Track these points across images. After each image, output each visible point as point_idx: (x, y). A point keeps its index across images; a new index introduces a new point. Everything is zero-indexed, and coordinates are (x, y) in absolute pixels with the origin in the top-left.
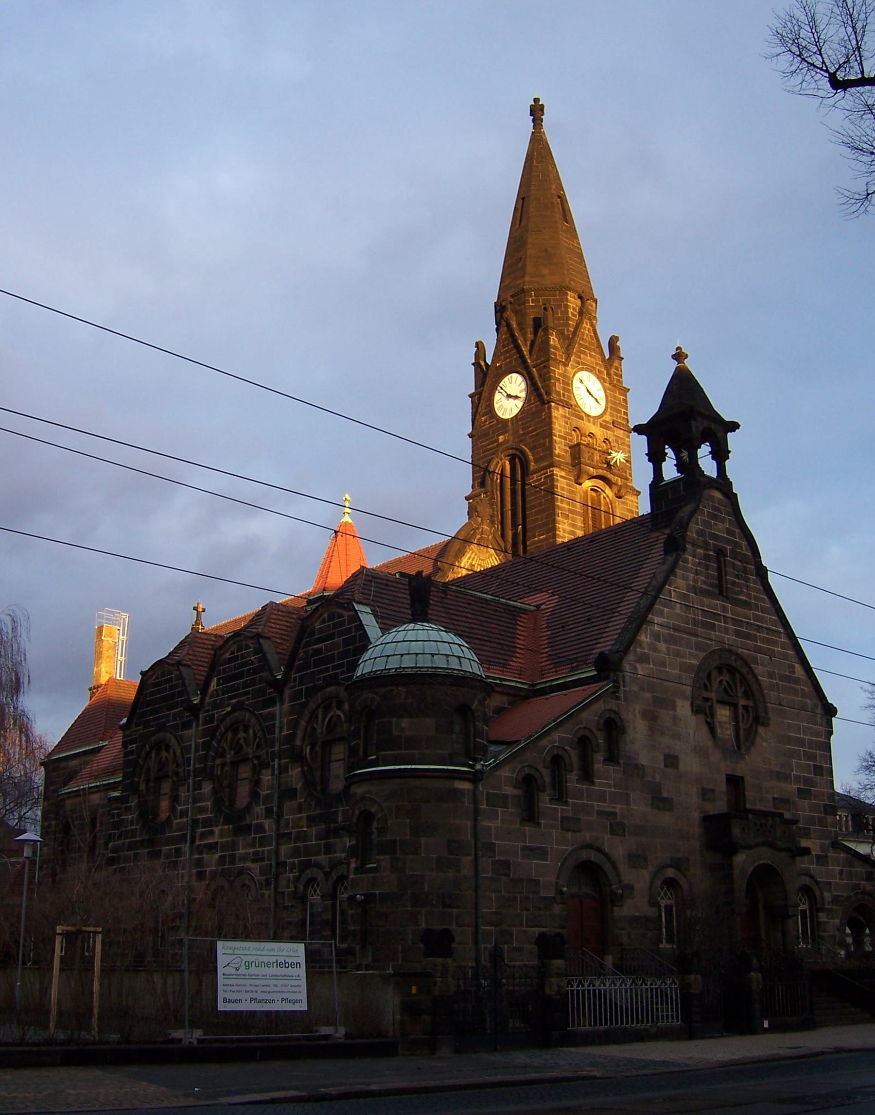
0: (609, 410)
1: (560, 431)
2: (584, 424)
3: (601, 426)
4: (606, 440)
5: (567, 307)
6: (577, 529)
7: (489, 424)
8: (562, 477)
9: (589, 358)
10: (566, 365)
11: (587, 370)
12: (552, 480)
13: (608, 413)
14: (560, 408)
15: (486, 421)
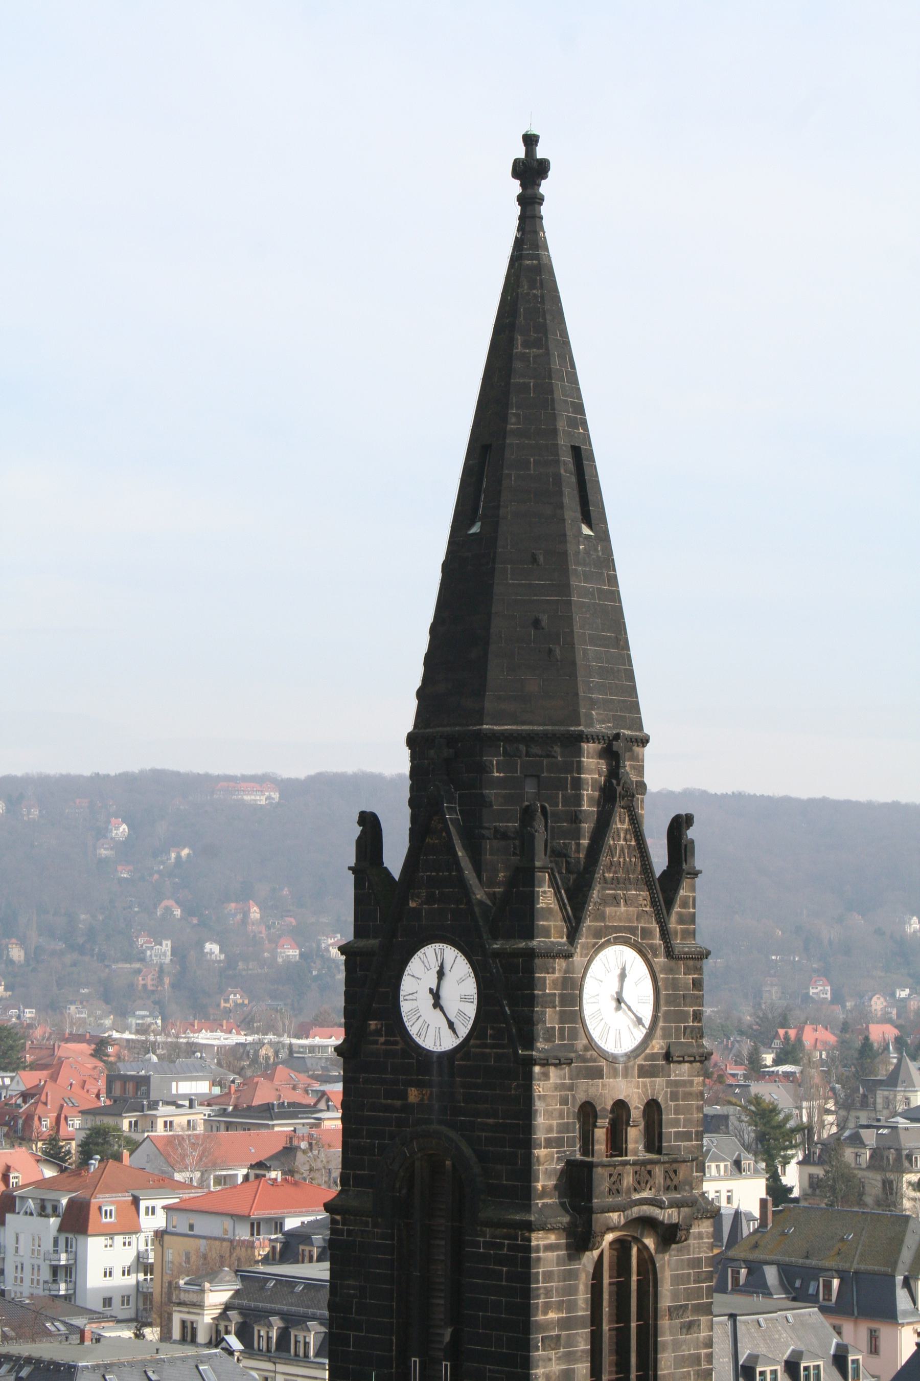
0: (661, 1024)
1: (550, 1129)
2: (603, 1085)
3: (644, 1072)
4: (653, 1108)
5: (578, 784)
6: (576, 1361)
7: (386, 1043)
8: (549, 1248)
9: (623, 909)
10: (568, 956)
11: (618, 941)
12: (527, 1263)
13: (659, 1032)
14: (552, 1071)
15: (378, 1032)
